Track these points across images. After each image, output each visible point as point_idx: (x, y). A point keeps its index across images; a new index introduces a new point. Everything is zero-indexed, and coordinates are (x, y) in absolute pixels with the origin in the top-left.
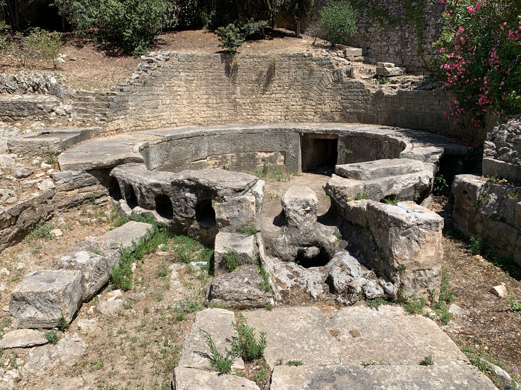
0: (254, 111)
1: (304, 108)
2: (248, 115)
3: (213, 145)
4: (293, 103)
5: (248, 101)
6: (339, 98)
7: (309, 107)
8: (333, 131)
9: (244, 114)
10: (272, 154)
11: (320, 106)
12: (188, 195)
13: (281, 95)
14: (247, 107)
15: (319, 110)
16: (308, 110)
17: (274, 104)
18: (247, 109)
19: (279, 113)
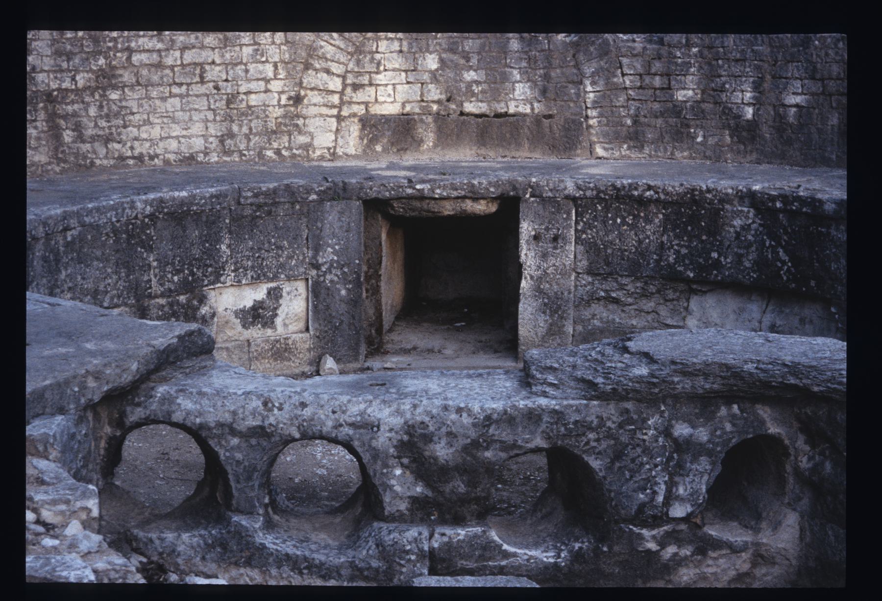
0: (103, 123)
1: (297, 100)
2: (80, 138)
3: (63, 275)
4: (253, 86)
5: (81, 83)
6: (432, 62)
7: (315, 97)
8: (496, 185)
9: (68, 136)
10: (259, 293)
11: (360, 96)
12: (682, 430)
13: (204, 53)
14: (76, 107)
15: (355, 108)
16: (313, 110)
17: (176, 90)
18: (75, 114)
19: (197, 128)
